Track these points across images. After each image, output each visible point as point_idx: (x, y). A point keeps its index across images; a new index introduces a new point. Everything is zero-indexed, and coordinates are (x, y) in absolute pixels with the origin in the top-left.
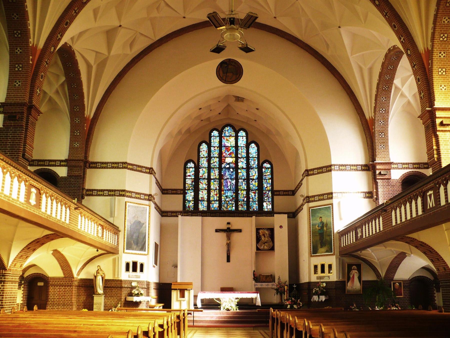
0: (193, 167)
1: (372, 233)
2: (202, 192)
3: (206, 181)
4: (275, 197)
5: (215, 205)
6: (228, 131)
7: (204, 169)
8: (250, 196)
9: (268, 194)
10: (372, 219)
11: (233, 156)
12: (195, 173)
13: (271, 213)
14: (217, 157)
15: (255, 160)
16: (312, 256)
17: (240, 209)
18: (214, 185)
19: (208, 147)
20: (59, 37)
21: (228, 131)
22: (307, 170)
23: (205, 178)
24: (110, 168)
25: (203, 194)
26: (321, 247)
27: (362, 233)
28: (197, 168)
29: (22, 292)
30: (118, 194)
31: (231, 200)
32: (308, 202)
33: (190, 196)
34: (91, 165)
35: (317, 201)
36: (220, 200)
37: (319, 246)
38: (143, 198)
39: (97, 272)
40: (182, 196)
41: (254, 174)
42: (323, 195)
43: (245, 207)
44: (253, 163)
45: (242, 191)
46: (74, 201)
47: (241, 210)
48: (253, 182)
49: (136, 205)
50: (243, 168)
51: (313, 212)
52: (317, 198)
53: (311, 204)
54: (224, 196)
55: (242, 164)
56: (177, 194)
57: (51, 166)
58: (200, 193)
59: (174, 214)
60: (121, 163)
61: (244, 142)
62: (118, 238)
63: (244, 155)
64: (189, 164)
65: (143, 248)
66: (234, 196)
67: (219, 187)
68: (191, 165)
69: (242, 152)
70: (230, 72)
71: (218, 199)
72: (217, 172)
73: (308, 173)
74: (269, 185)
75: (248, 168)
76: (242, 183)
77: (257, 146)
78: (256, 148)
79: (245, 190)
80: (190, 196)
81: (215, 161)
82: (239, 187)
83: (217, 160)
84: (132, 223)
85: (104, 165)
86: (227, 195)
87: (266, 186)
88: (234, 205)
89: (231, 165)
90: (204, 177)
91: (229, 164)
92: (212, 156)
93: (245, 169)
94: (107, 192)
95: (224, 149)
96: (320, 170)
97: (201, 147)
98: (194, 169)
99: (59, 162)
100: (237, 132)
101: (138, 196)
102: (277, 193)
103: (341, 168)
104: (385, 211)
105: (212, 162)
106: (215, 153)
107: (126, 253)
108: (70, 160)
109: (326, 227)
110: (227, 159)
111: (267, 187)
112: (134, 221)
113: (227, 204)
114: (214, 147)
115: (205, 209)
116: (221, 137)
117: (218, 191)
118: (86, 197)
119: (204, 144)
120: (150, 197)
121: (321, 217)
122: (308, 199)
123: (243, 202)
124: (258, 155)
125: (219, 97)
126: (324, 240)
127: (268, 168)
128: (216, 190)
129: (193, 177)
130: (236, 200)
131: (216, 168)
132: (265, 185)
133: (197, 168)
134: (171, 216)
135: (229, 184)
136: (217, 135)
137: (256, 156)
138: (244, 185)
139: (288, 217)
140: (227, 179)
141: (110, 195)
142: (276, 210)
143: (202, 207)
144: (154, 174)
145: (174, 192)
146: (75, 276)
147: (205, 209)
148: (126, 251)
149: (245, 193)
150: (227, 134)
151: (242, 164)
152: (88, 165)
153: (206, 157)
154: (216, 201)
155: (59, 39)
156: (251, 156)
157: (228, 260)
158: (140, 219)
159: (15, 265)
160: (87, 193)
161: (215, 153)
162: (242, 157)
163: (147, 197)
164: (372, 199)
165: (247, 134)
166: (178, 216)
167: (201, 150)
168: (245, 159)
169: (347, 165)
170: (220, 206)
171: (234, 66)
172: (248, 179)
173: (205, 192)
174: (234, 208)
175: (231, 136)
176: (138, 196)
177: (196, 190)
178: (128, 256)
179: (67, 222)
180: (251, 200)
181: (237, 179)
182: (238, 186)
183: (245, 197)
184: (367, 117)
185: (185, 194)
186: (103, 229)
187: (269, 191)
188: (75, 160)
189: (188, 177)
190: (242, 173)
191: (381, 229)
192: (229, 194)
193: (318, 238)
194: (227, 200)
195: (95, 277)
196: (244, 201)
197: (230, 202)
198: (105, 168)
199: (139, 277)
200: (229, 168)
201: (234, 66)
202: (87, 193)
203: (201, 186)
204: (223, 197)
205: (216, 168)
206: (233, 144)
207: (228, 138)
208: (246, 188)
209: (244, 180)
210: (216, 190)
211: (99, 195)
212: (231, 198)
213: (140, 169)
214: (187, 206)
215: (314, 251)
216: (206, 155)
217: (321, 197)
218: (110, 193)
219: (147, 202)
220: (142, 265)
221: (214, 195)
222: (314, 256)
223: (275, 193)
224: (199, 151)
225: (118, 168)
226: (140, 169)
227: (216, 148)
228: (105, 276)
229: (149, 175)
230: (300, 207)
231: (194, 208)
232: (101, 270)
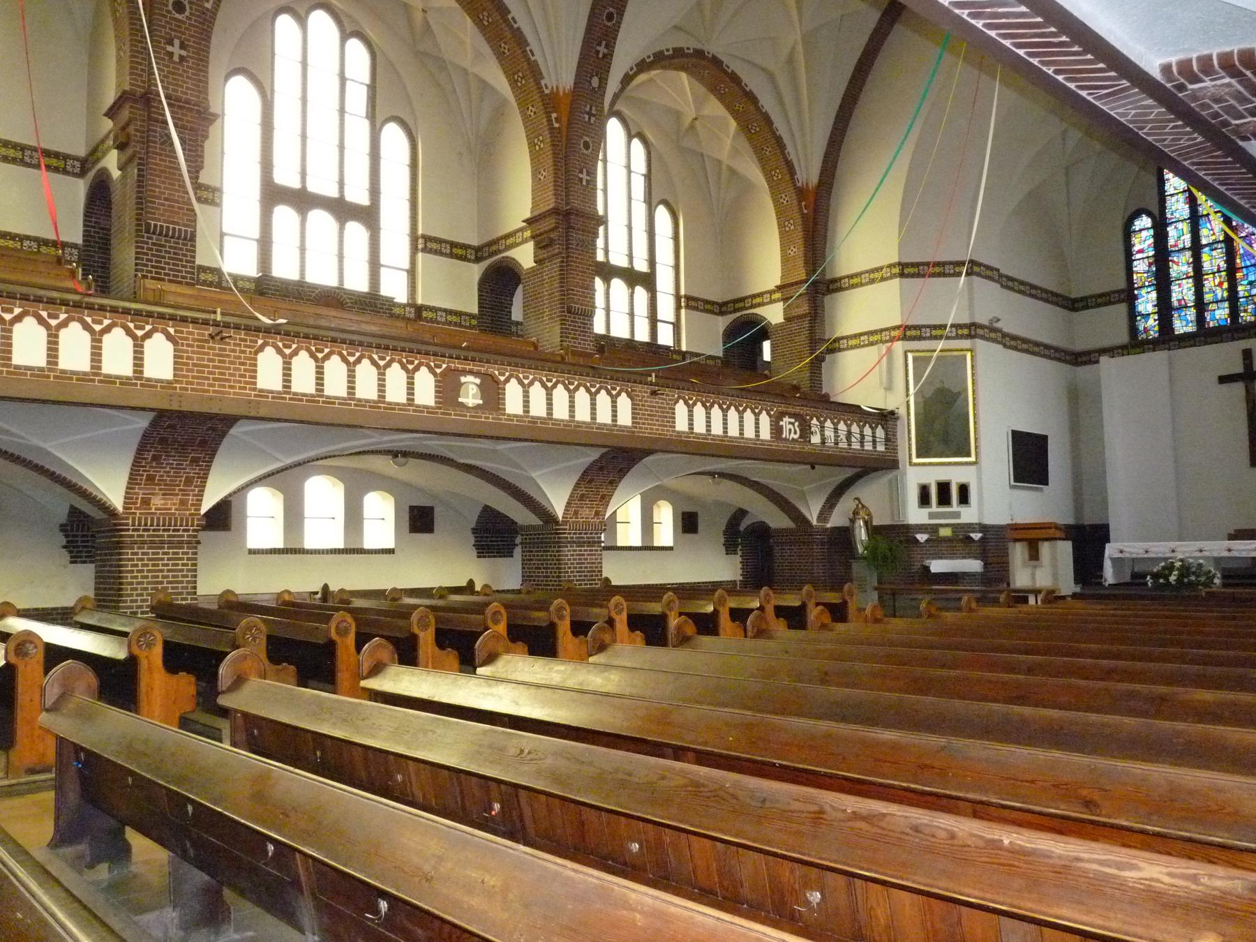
3: (1188, 254)
5: (1220, 314)
7: (1180, 225)
18: (1213, 260)
20: (602, 49)
23: (1184, 249)
24: (867, 284)
25: (1183, 291)
29: (740, 559)
33: (1147, 302)
36: (1233, 297)
39: (855, 513)
40: (1122, 308)
54: (1245, 282)
57: (753, 306)
58: (1174, 288)
64: (1137, 223)
67: (1226, 262)
68: (1144, 222)
71: (1226, 294)
80: (1147, 302)
85: (855, 281)
90: (1181, 246)
107: (916, 465)
115: (1191, 328)
120: (972, 330)
128: (1219, 271)
129: (1152, 253)
141: (872, 344)
143: (1183, 324)
145: (1104, 299)
146: (815, 523)
148: (915, 460)
152: (822, 287)
154: (1222, 300)
155: (605, 56)
159: (576, 513)
163: (966, 331)
166: (1097, 362)
170: (1234, 312)
177: (1163, 283)
178: (919, 471)
189: (1138, 256)
195: (853, 521)
199: (957, 515)
203: (1174, 271)
204: (1240, 288)
210: (1219, 271)
211: (852, 348)
214: (1141, 328)
218: (872, 339)
219: (966, 343)
220: (964, 490)
221: (1215, 287)
228: (871, 518)
231: (1160, 331)
232: (863, 506)
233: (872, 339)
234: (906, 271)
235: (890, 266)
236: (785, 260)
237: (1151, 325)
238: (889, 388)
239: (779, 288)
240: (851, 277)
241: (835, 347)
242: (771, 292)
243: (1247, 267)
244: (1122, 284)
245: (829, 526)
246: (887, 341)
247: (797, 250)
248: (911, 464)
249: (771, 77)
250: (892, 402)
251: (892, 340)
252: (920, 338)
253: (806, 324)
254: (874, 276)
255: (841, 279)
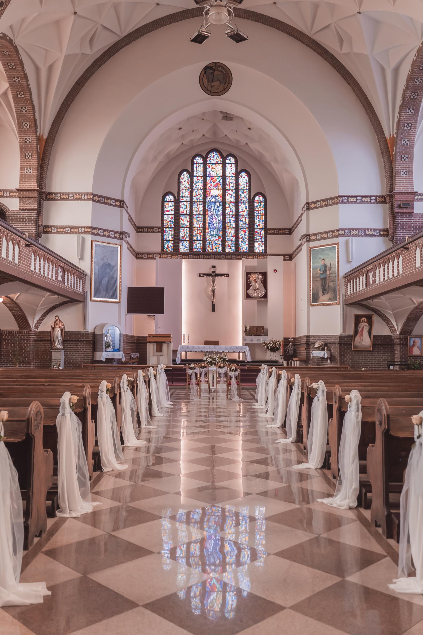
0: (173, 200)
1: (389, 277)
2: (184, 230)
3: (188, 217)
4: (268, 236)
6: (214, 157)
7: (185, 204)
8: (239, 235)
9: (260, 233)
10: (389, 260)
11: (220, 187)
12: (175, 208)
13: (264, 255)
14: (200, 189)
15: (246, 192)
16: (312, 305)
17: (227, 250)
18: (198, 222)
19: (190, 177)
21: (214, 157)
22: (308, 203)
24: (72, 200)
25: (184, 233)
26: (323, 294)
27: (375, 277)
28: (177, 202)
30: (83, 231)
31: (217, 240)
32: (308, 241)
33: (169, 235)
34: (48, 197)
35: (319, 240)
36: (204, 240)
37: (321, 293)
38: (113, 236)
40: (160, 234)
41: (244, 209)
42: (327, 232)
43: (234, 248)
44: (243, 196)
45: (230, 229)
46: (24, 236)
47: (229, 252)
48: (243, 219)
49: (105, 244)
50: (231, 202)
51: (312, 254)
52: (319, 237)
53: (312, 244)
54: (209, 235)
55: (230, 197)
56: (154, 232)
58: (181, 231)
59: (150, 256)
60: (85, 194)
61: (234, 171)
62: (84, 283)
63: (233, 186)
65: (114, 296)
66: (220, 235)
68: (170, 198)
69: (231, 183)
70: (216, 79)
71: (202, 238)
72: (200, 206)
73: (309, 206)
74: (261, 222)
75: (237, 202)
76: (230, 220)
77: (248, 176)
78: (247, 178)
79: (233, 228)
81: (198, 194)
82: (226, 225)
83: (201, 192)
84: (100, 265)
85: (65, 197)
86: (212, 233)
87: (258, 224)
88: (220, 246)
89: (217, 198)
90: (185, 213)
91: (214, 197)
92: (194, 187)
93: (233, 202)
94: (69, 229)
95: (208, 180)
96: (324, 203)
97: (182, 177)
98: (173, 203)
99: (8, 193)
100: (224, 159)
101: (107, 233)
102: (271, 231)
103: (350, 199)
104: (408, 249)
105: (195, 195)
106: (199, 184)
108: (22, 190)
109: (330, 270)
110: (212, 191)
111: (259, 225)
112: (102, 263)
113: (213, 244)
114: (198, 177)
115: (187, 250)
116: (205, 164)
117: (201, 229)
118: (43, 235)
119: (185, 173)
121: (324, 259)
122: (307, 237)
123: (231, 242)
124: (250, 186)
125: (204, 114)
126: (327, 286)
127: (261, 202)
128: (200, 228)
129: (173, 213)
130: (224, 241)
131: (200, 202)
132: (257, 222)
133: (177, 202)
134: (147, 258)
135: (215, 221)
136: (201, 162)
137: (247, 188)
138: (232, 222)
139: (284, 260)
140: (212, 215)
141: (73, 233)
142: (269, 252)
143: (184, 247)
144: (126, 208)
145: (151, 230)
146: (33, 328)
147: (187, 250)
148: (94, 299)
149: (233, 231)
150: (213, 161)
151: (230, 197)
152: (44, 196)
153: (188, 189)
156: (240, 187)
157: (213, 310)
158: (109, 261)
160: (45, 230)
161: (199, 184)
162: (230, 189)
163: (118, 235)
164: (387, 239)
165: (236, 161)
167: (181, 180)
168: (234, 191)
169: (359, 196)
171: (221, 71)
172: (237, 215)
173: (187, 230)
174: (220, 249)
175: (216, 163)
176: (107, 233)
177: (177, 228)
179: (16, 261)
180: (240, 240)
181: (224, 215)
182: (225, 223)
183: (233, 236)
184: (387, 135)
185: (163, 232)
186: (64, 272)
187: (262, 229)
188: (28, 190)
189: (167, 213)
190: (230, 208)
191: (401, 272)
192: (215, 232)
193: (319, 284)
194: (212, 239)
196: (232, 241)
197: (216, 242)
198: (65, 200)
200: (215, 202)
201: (221, 71)
202: (45, 230)
203: (182, 223)
204: (207, 237)
205: (200, 202)
206: (220, 173)
207: (213, 166)
208: (234, 226)
209: (233, 215)
211: (60, 233)
212: (217, 237)
213: (108, 201)
214: (166, 246)
215: (314, 299)
216: (188, 186)
217: (325, 236)
218: (72, 230)
219: (118, 241)
221: (197, 234)
222: (314, 305)
223: (269, 232)
224: (179, 182)
225: (82, 199)
226: (108, 201)
227: (200, 178)
229: (119, 209)
230: (298, 248)
233: (72, 230)
234: (95, 198)
235: (88, 194)
236: (23, 175)
237: (169, 246)
238: (81, 258)
239: (18, 190)
240: (63, 194)
241: (47, 230)
242: (12, 191)
243: (210, 228)
244: (160, 225)
245: (38, 330)
246: (82, 233)
247: (33, 171)
248: (91, 300)
249: (37, 70)
250: (85, 266)
251: (86, 233)
252: (98, 235)
253: (34, 214)
254: (78, 197)
255: (55, 194)
